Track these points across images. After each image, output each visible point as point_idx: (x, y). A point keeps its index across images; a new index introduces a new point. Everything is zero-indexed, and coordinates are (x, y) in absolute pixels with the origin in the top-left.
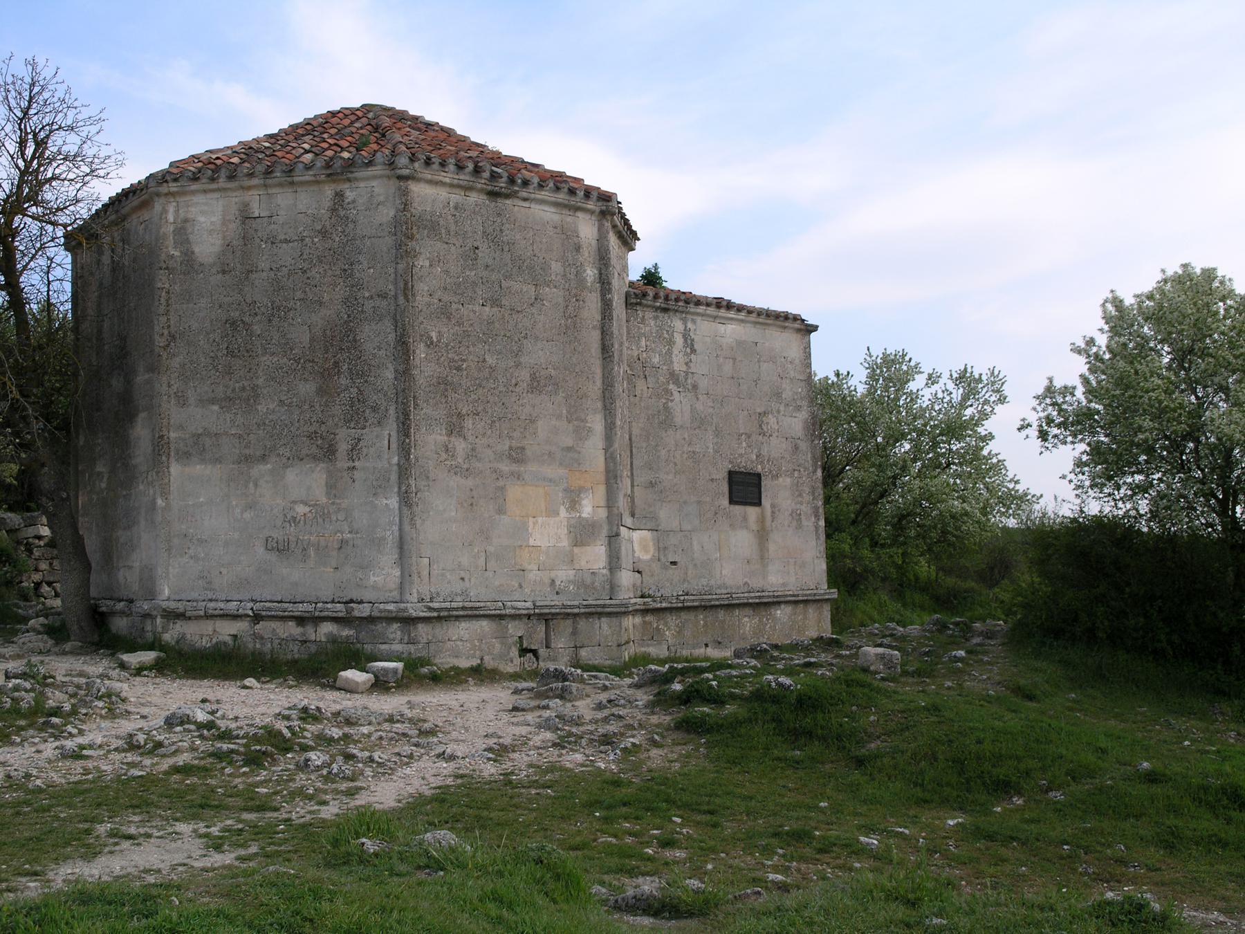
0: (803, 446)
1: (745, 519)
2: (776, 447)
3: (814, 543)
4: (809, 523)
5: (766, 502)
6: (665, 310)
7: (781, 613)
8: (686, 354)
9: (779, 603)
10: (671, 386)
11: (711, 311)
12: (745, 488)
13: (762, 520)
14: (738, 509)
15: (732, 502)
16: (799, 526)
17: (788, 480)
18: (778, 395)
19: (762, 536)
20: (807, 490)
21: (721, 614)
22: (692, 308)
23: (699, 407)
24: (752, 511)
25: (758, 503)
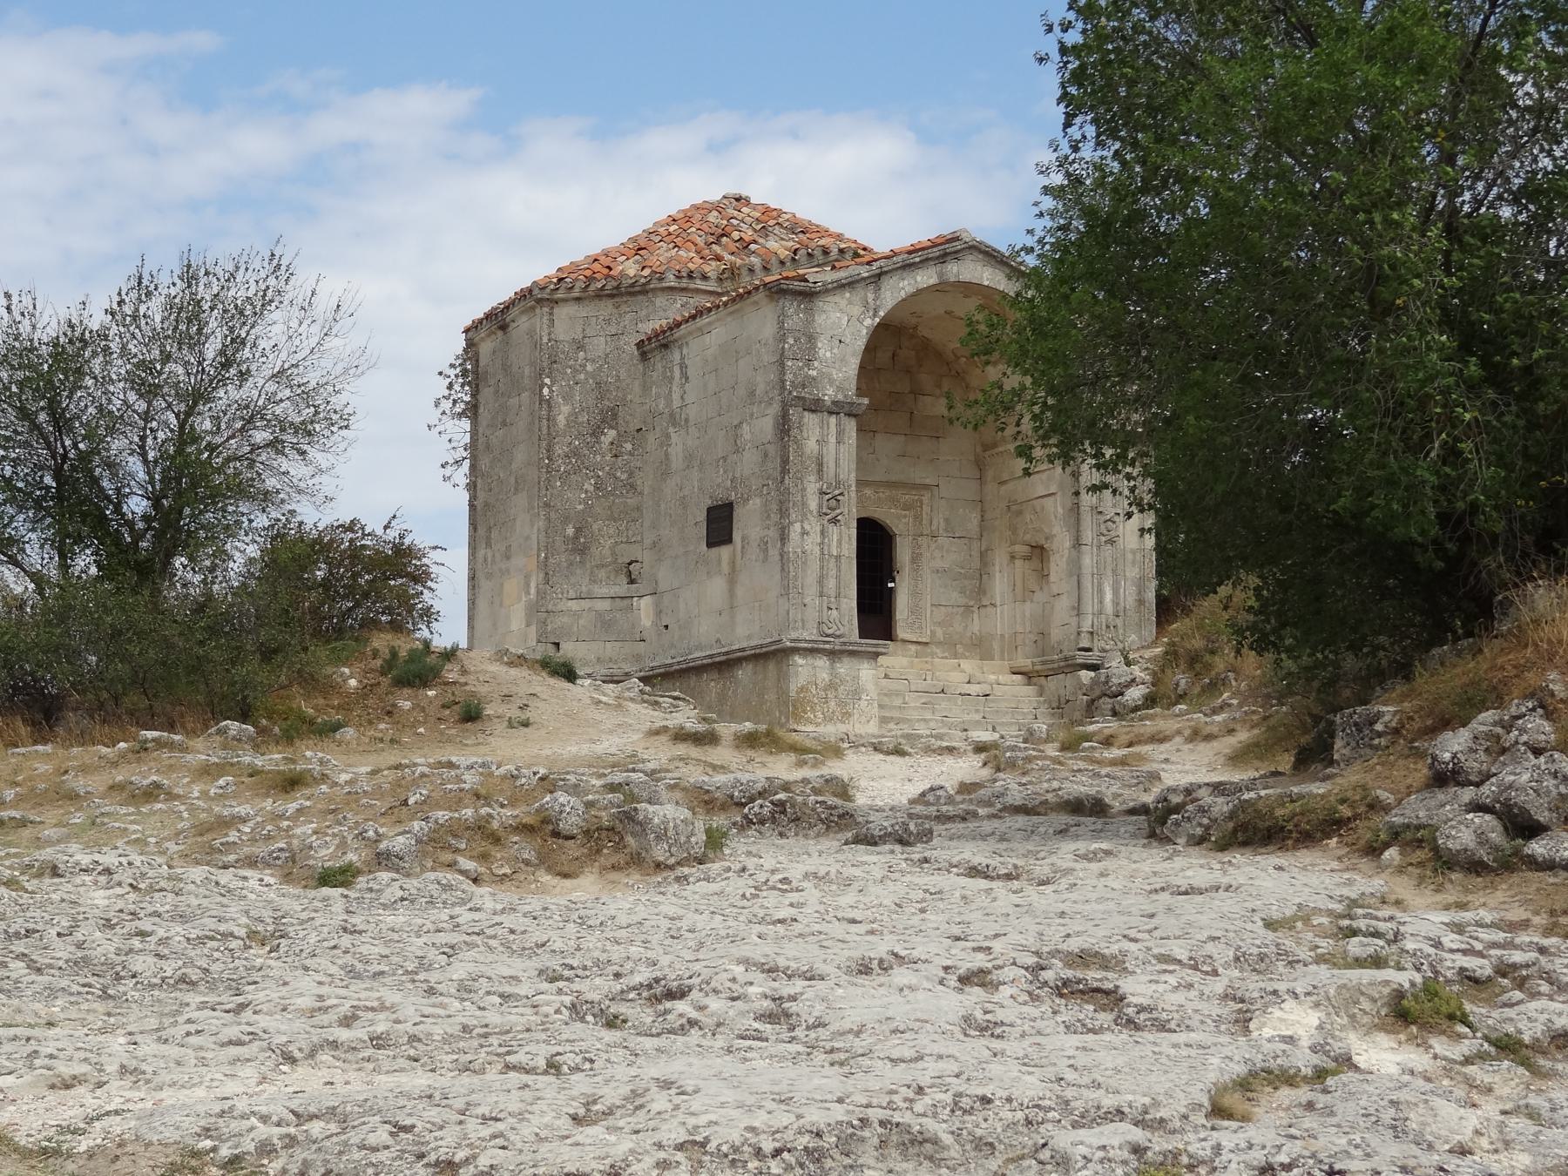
0: (772, 449)
1: (719, 561)
2: (749, 462)
3: (778, 577)
4: (774, 553)
5: (737, 536)
6: (666, 346)
7: (743, 674)
8: (682, 386)
9: (739, 660)
10: (671, 430)
11: (691, 326)
12: (720, 524)
13: (733, 563)
14: (715, 550)
15: (710, 545)
16: (765, 560)
17: (758, 501)
18: (752, 393)
19: (732, 581)
20: (775, 507)
21: (693, 679)
22: (677, 334)
23: (690, 443)
24: (724, 551)
25: (729, 540)
